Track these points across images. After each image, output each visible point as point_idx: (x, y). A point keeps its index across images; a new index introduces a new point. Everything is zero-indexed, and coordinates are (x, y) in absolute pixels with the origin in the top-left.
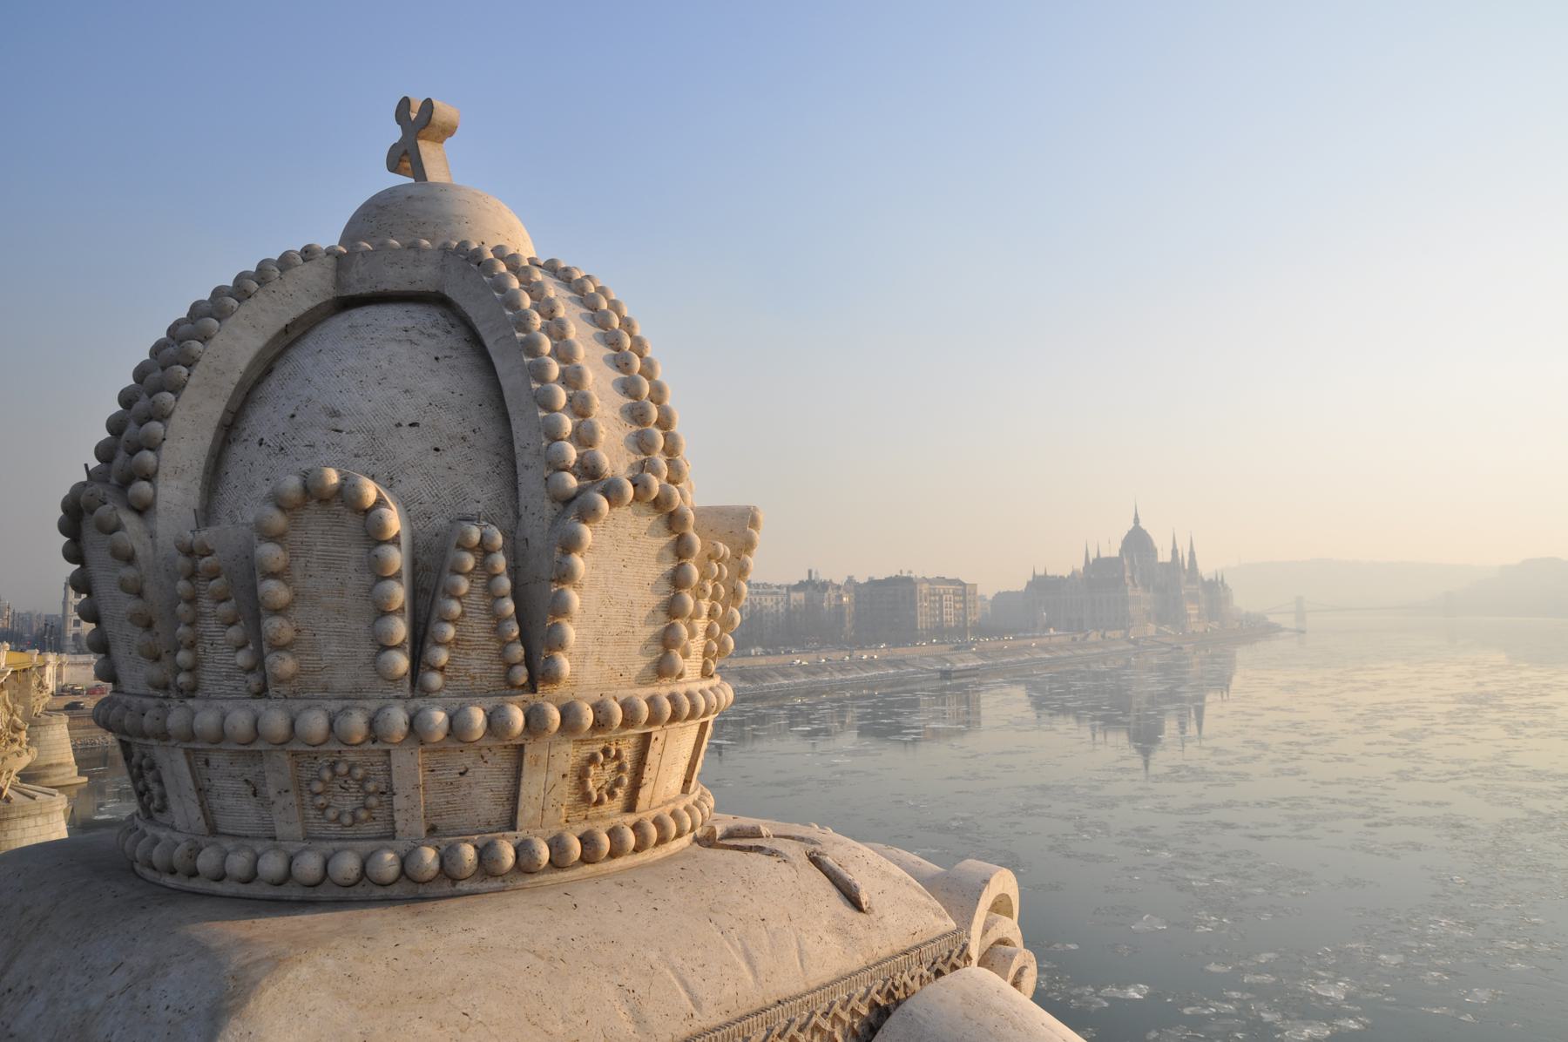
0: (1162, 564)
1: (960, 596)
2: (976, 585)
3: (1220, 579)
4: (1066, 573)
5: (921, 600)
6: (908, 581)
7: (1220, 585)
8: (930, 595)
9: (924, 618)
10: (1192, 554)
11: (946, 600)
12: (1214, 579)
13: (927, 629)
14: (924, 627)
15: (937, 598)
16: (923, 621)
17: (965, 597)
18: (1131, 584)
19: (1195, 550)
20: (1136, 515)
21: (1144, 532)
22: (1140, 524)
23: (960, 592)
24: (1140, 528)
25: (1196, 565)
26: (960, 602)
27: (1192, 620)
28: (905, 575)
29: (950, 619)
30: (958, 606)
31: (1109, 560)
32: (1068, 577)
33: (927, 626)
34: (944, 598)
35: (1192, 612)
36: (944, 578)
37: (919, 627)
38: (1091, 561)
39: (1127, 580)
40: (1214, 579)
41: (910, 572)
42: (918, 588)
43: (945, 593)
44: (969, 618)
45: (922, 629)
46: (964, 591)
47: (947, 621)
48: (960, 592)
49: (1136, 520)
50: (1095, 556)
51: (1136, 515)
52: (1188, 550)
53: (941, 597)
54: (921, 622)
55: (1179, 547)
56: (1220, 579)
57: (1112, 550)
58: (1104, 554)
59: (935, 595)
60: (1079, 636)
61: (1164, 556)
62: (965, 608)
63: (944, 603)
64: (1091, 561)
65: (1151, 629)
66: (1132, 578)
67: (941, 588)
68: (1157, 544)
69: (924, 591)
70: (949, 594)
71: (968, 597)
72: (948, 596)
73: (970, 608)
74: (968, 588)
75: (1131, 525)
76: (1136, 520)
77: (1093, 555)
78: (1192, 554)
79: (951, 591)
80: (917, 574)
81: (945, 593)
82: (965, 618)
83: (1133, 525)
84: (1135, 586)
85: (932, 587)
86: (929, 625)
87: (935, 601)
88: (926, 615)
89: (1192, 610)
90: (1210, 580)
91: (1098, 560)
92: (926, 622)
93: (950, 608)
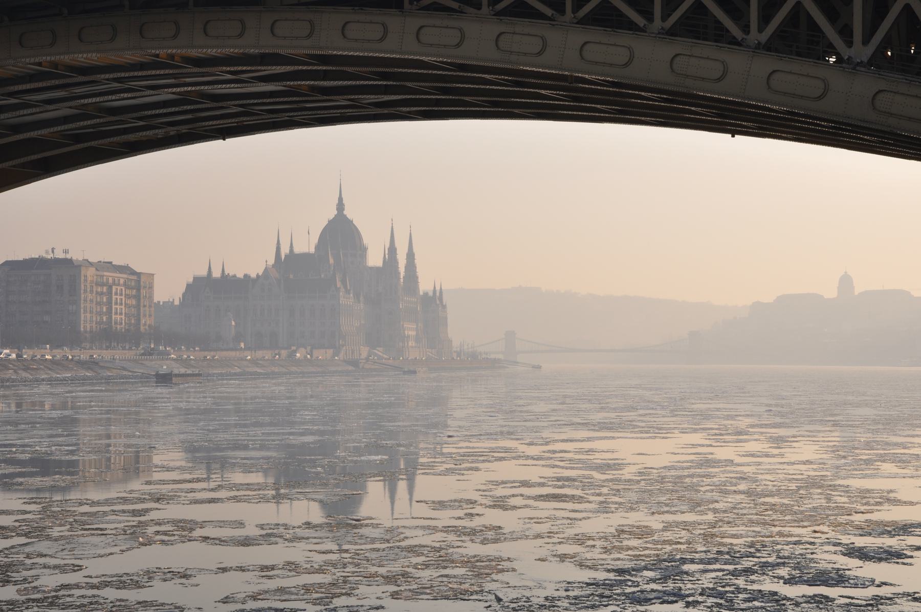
0: (371, 268)
1: (132, 288)
2: (153, 275)
3: (438, 294)
4: (255, 269)
5: (85, 291)
6: (68, 262)
7: (438, 302)
8: (97, 284)
9: (88, 315)
10: (411, 256)
11: (116, 294)
12: (431, 294)
13: (91, 332)
14: (88, 330)
15: (105, 289)
16: (87, 321)
17: (138, 290)
18: (343, 290)
19: (416, 250)
20: (341, 199)
21: (350, 222)
22: (345, 212)
23: (133, 284)
24: (345, 216)
25: (415, 271)
26: (134, 297)
27: (410, 344)
28: (60, 255)
29: (120, 318)
30: (129, 302)
31: (305, 256)
32: (258, 275)
33: (91, 327)
34: (114, 290)
35: (410, 333)
36: (111, 263)
37: (82, 329)
38: (283, 257)
39: (339, 284)
40: (431, 294)
41: (66, 252)
42: (83, 273)
43: (114, 284)
44: (143, 321)
45: (86, 332)
46: (139, 281)
47: (116, 323)
48: (133, 284)
49: (340, 206)
50: (288, 251)
51: (341, 199)
52: (406, 251)
53: (110, 287)
54: (85, 321)
55: (397, 245)
56: (438, 294)
57: (306, 244)
58: (297, 250)
59: (102, 285)
60: (284, 353)
61: (375, 259)
62: (138, 306)
63: (114, 297)
64: (283, 257)
65: (365, 351)
66: (344, 282)
67: (109, 276)
68: (367, 240)
69: (89, 279)
70: (119, 285)
71: (143, 292)
72: (119, 288)
73: (145, 306)
74: (143, 280)
75: (332, 213)
76: (340, 206)
77: (285, 250)
78: (411, 256)
79: (122, 281)
80: (76, 255)
81: (114, 284)
82: (138, 320)
83: (336, 212)
84: (347, 292)
85: (99, 273)
86: (94, 325)
87: (102, 293)
88: (91, 312)
89: (410, 330)
90: (426, 294)
91: (291, 255)
92: (91, 321)
93: (121, 304)
